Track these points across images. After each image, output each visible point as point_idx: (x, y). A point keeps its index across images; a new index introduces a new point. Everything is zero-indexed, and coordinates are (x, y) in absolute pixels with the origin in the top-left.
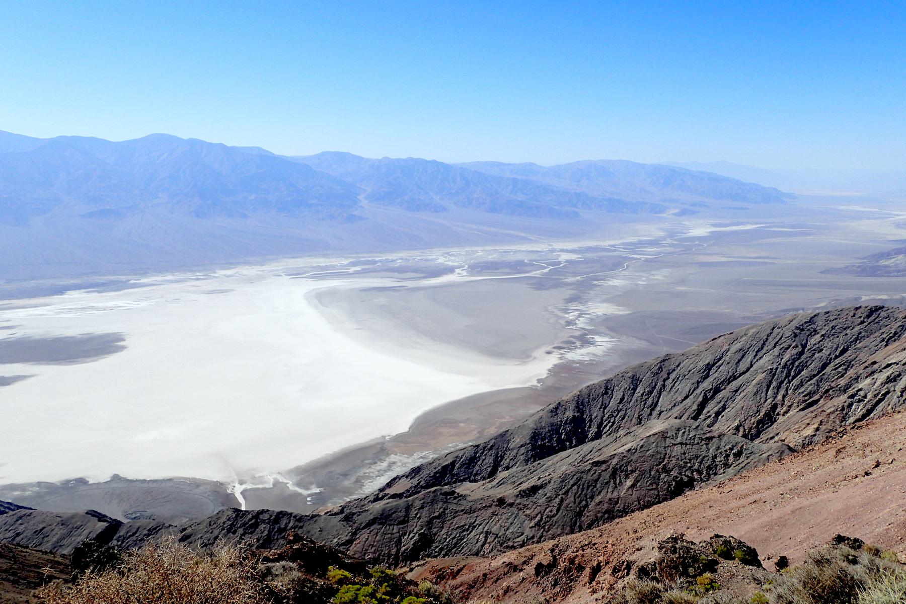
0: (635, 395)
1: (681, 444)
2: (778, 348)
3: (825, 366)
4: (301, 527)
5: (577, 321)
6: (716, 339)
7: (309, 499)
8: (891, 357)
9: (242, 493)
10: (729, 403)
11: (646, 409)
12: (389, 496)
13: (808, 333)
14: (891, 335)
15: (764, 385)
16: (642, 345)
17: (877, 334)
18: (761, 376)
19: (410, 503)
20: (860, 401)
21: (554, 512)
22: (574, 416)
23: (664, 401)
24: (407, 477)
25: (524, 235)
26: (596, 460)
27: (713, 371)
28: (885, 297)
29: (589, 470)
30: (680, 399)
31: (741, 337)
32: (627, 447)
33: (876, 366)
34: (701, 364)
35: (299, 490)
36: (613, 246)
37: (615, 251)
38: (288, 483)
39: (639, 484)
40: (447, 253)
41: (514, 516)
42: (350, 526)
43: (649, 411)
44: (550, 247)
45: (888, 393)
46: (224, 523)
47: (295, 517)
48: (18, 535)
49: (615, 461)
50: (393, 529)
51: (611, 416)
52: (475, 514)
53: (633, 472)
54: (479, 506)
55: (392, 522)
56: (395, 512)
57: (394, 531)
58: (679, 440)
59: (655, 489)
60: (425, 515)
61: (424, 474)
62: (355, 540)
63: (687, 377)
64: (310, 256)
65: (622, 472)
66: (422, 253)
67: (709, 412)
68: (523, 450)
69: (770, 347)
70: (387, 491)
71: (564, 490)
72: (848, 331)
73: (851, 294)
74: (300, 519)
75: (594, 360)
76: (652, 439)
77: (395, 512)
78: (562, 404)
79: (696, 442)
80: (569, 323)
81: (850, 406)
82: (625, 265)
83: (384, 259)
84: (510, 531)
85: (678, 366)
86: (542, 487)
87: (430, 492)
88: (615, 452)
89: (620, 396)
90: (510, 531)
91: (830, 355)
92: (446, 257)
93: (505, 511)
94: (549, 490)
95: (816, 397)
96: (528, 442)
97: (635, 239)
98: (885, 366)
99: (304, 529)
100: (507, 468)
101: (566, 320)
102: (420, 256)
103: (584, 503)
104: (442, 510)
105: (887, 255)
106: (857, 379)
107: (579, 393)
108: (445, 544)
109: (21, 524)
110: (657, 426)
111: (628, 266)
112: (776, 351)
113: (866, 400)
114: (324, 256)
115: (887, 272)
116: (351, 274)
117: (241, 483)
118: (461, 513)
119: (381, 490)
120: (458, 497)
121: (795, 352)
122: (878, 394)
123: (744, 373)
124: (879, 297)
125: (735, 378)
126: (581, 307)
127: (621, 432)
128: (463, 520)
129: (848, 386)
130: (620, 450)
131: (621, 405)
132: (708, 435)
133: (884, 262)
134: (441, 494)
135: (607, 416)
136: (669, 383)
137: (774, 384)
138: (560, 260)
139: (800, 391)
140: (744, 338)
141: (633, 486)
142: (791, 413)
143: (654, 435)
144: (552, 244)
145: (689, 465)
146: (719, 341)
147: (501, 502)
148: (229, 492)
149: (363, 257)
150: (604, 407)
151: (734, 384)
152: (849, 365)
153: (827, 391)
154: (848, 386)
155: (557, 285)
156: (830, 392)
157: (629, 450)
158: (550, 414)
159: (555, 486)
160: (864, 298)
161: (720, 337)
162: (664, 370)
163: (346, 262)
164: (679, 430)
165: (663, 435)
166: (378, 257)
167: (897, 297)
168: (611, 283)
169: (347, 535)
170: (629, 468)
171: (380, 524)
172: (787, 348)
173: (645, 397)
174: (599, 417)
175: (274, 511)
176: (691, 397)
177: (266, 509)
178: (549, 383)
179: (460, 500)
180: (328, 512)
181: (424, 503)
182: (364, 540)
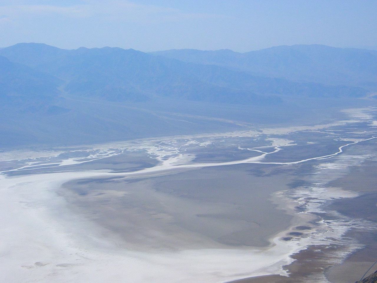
36: (324, 130)
37: (327, 135)
40: (158, 142)
44: (260, 133)
66: (132, 143)
80: (301, 209)
82: (340, 148)
83: (94, 150)
92: (158, 146)
97: (343, 123)
101: (296, 206)
102: (131, 146)
138: (273, 145)
144: (261, 130)
149: (73, 149)
163: (56, 155)
166: (88, 148)
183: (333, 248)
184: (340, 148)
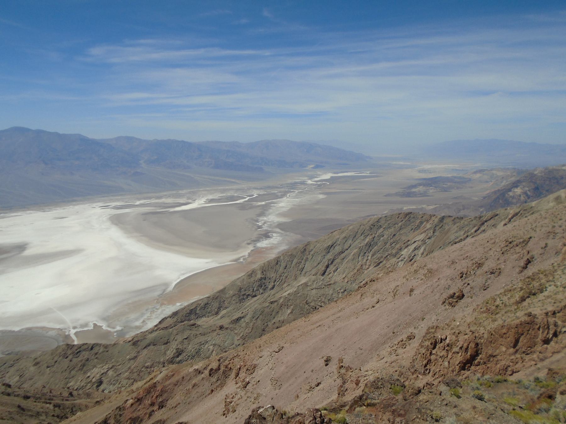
0: (293, 264)
1: (316, 288)
2: (363, 236)
3: (386, 243)
4: (107, 351)
5: (263, 226)
6: (332, 233)
7: (115, 334)
8: (416, 237)
10: (340, 265)
11: (298, 271)
12: (160, 329)
13: (377, 227)
14: (416, 226)
15: (357, 255)
16: (299, 237)
17: (409, 227)
18: (356, 251)
19: (171, 333)
20: (402, 260)
21: (250, 330)
22: (261, 277)
23: (308, 266)
24: (170, 317)
25: (234, 180)
26: (271, 300)
27: (332, 248)
28: (414, 207)
29: (268, 306)
30: (316, 265)
31: (345, 231)
32: (287, 293)
33: (409, 242)
34: (326, 246)
35: (109, 329)
36: (281, 185)
37: (282, 188)
39: (294, 312)
41: (228, 334)
42: (136, 348)
43: (300, 272)
45: (415, 255)
46: (60, 353)
47: (103, 346)
49: (281, 300)
50: (161, 348)
51: (280, 276)
52: (207, 335)
53: (292, 305)
54: (209, 331)
55: (160, 344)
56: (161, 338)
57: (162, 349)
58: (314, 287)
59: (302, 313)
60: (180, 338)
61: (181, 314)
62: (140, 355)
63: (319, 253)
64: (112, 196)
65: (285, 306)
67: (330, 271)
68: (234, 298)
69: (359, 235)
70: (159, 326)
71: (255, 318)
72: (396, 226)
73: (399, 206)
74: (106, 347)
75: (273, 246)
76: (300, 287)
77: (161, 338)
78: (255, 271)
79: (323, 287)
80: (260, 227)
81: (398, 262)
84: (227, 343)
85: (314, 247)
86: (243, 317)
87: (182, 325)
88: (281, 296)
89: (284, 266)
90: (227, 343)
91: (388, 238)
93: (224, 332)
94: (247, 319)
95: (382, 260)
96: (237, 293)
98: (413, 242)
99: (110, 352)
100: (226, 308)
103: (266, 324)
104: (189, 334)
105: (415, 186)
106: (401, 249)
107: (263, 265)
108: (191, 353)
110: (303, 280)
111: (289, 196)
112: (362, 237)
113: (405, 260)
114: (121, 195)
115: (414, 195)
116: (137, 205)
117: (74, 328)
118: (199, 335)
119: (156, 326)
120: (197, 327)
121: (371, 237)
122: (411, 256)
123: (347, 250)
124: (411, 207)
125: (342, 252)
126: (265, 218)
127: (285, 285)
128: (202, 339)
129: (397, 253)
130: (284, 294)
131: (285, 270)
132: (329, 283)
133: (414, 190)
134: (188, 326)
135: (278, 276)
136: (310, 257)
137: (362, 254)
139: (374, 257)
140: (346, 231)
141: (291, 312)
142: (370, 268)
143: (301, 285)
145: (319, 299)
146: (334, 233)
147: (221, 328)
148: (67, 334)
150: (276, 271)
151: (343, 255)
152: (396, 242)
153: (387, 256)
154: (397, 253)
155: (252, 207)
156: (388, 256)
157: (289, 294)
158: (248, 277)
159: (251, 316)
160: (405, 208)
161: (334, 231)
162: (307, 250)
164: (314, 281)
165: (306, 285)
167: (420, 207)
168: (280, 205)
169: (134, 353)
170: (289, 304)
171: (154, 345)
172: (368, 236)
173: (298, 265)
174: (274, 278)
175: (90, 344)
176: (321, 263)
177: (85, 342)
178: (249, 260)
179: (198, 328)
180: (125, 341)
181: (178, 332)
182: (145, 355)
183: (271, 248)
184: (288, 195)
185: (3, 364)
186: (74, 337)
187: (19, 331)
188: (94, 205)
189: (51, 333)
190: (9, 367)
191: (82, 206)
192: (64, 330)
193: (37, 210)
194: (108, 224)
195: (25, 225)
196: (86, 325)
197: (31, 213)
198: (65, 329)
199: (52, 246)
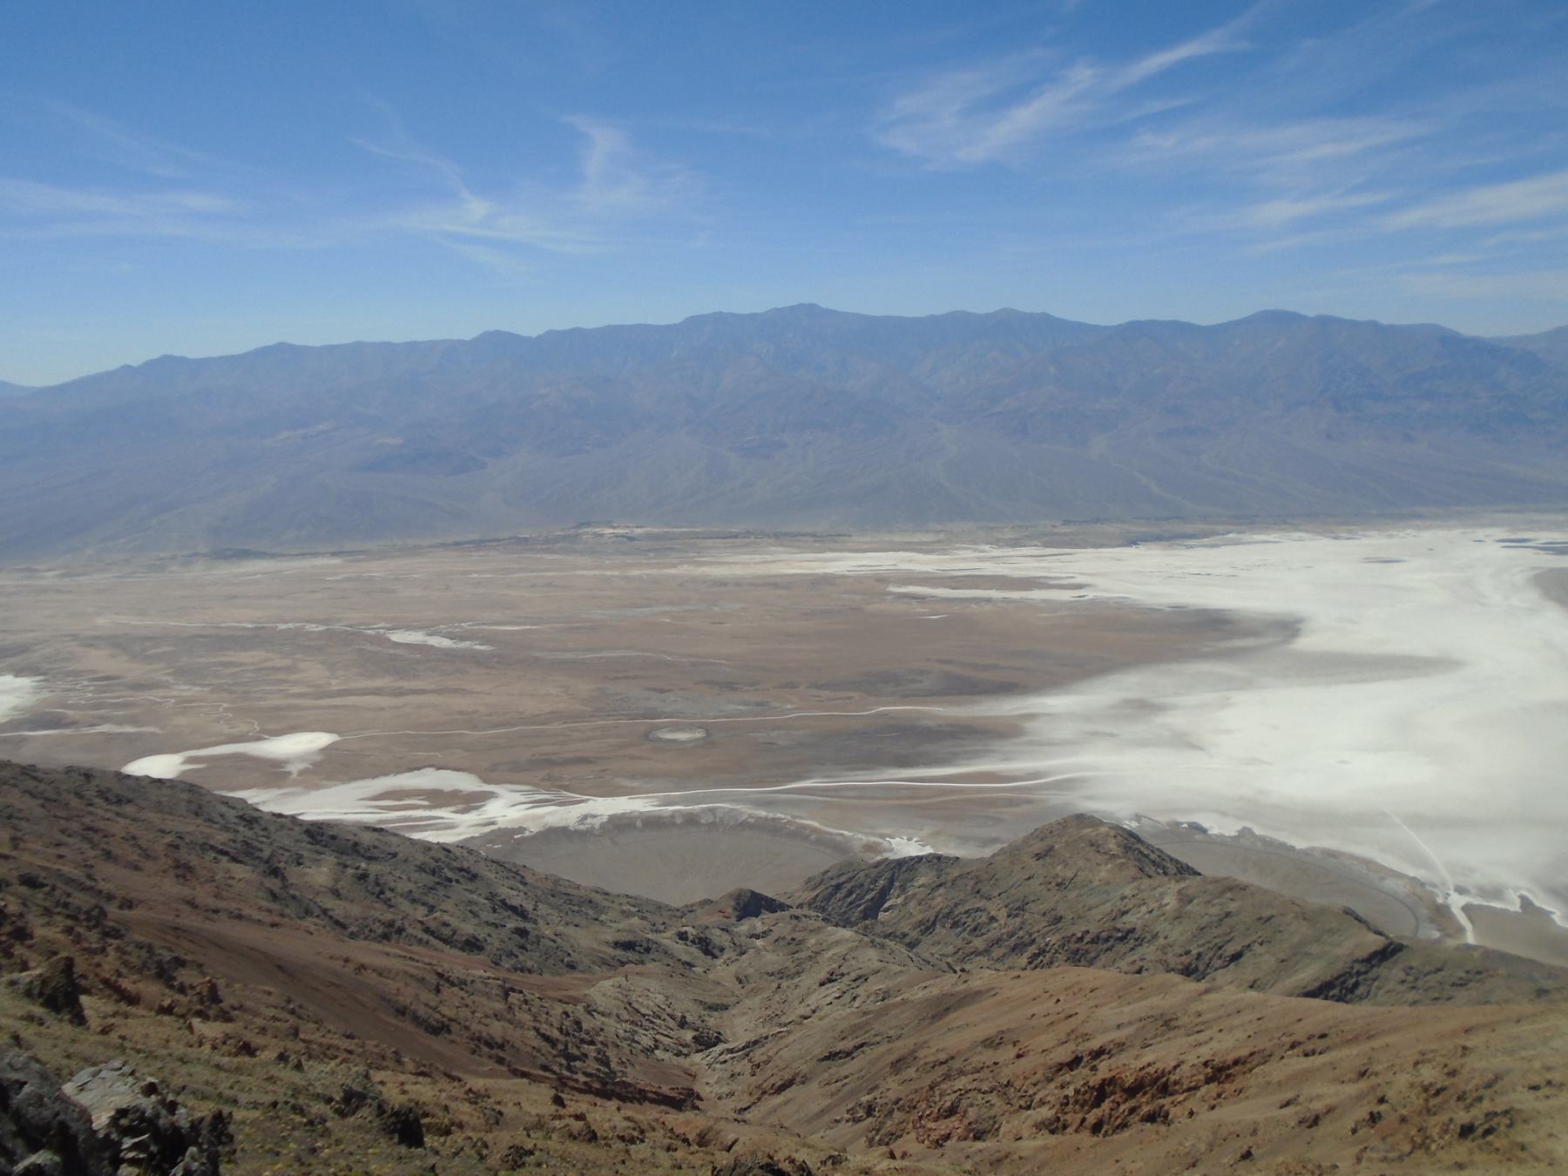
9: (1467, 909)
38: (1552, 913)
48: (1228, 915)
64: (1534, 511)
109: (1232, 900)
117: (1461, 890)
148: (1440, 900)
185: (1433, 969)
186: (1462, 919)
187: (1306, 852)
188: (1480, 533)
189: (1390, 884)
190: (1453, 985)
191: (1442, 533)
192: (1428, 888)
193: (1320, 534)
194: (1532, 596)
195: (1290, 569)
196: (1497, 893)
197: (1301, 540)
198: (1434, 885)
199: (1369, 636)
